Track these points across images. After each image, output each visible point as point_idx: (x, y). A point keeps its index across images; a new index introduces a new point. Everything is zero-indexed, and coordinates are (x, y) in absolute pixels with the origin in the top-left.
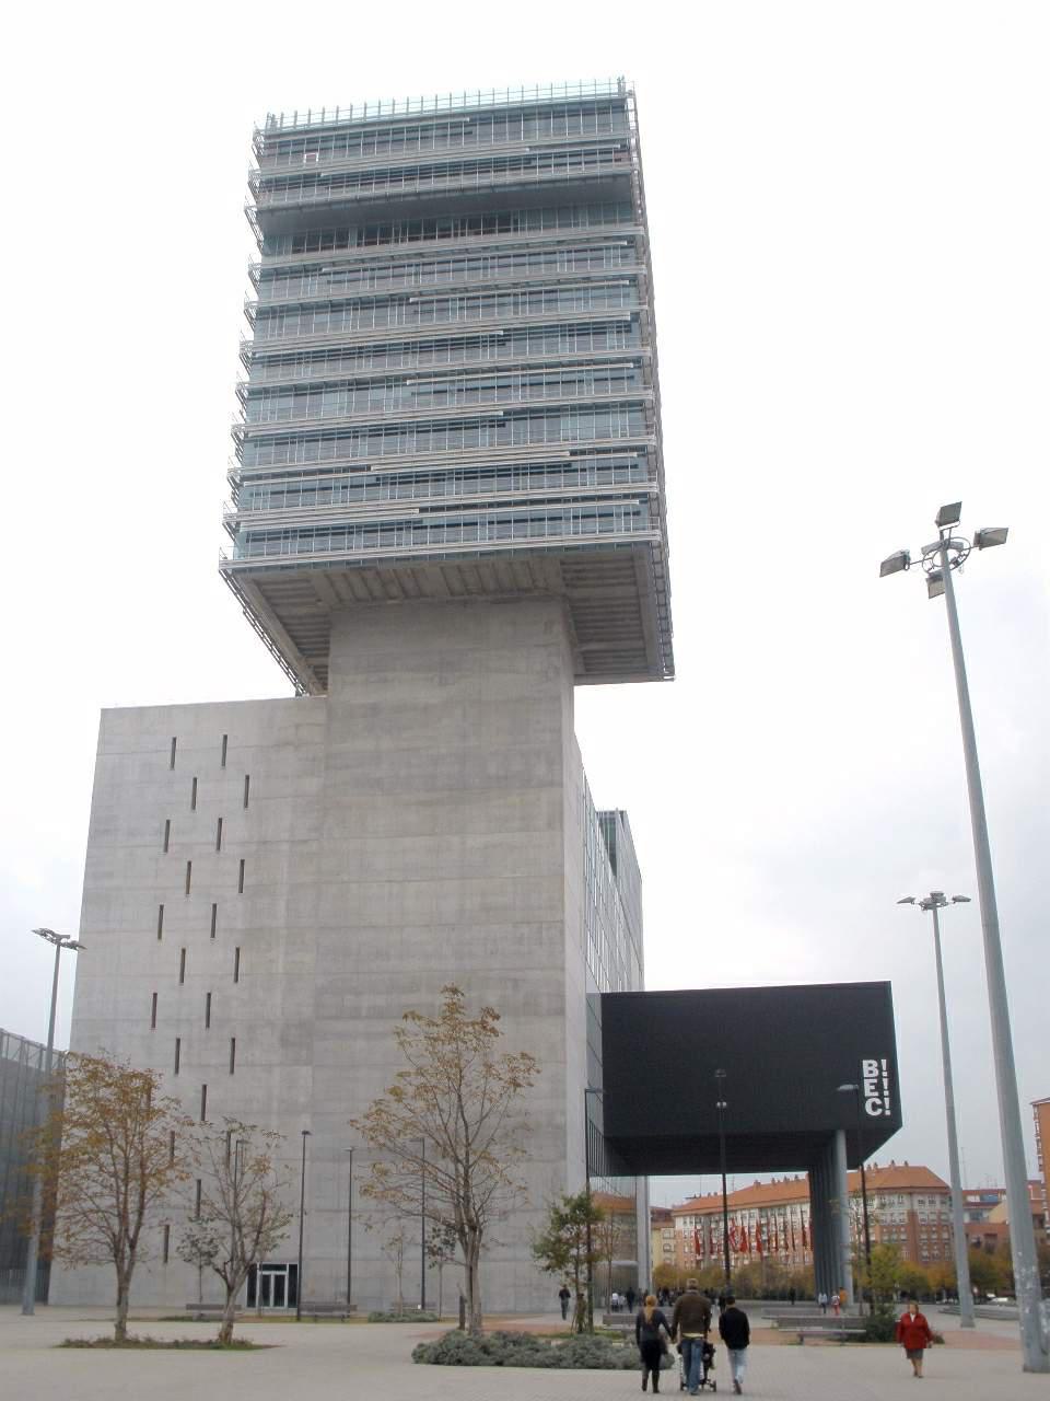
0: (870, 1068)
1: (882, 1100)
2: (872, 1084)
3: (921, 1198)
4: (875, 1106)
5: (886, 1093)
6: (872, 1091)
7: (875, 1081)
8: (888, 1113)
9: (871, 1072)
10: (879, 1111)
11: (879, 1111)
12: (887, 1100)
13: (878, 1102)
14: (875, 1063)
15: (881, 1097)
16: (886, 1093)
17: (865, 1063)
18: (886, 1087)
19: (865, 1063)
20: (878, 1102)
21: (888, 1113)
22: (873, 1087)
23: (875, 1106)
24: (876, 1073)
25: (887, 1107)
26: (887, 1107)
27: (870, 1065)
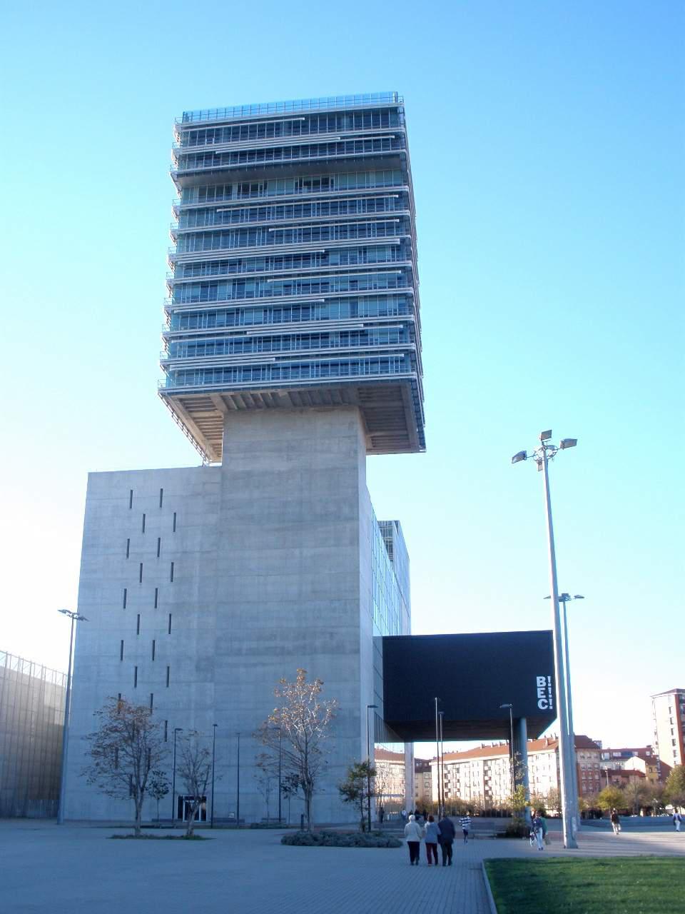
0: (541, 682)
1: (548, 700)
3: (582, 754)
4: (543, 704)
5: (550, 696)
6: (542, 695)
7: (544, 689)
8: (551, 708)
9: (541, 684)
10: (546, 707)
11: (546, 707)
12: (551, 700)
13: (546, 701)
14: (544, 678)
15: (547, 698)
16: (550, 696)
17: (538, 678)
19: (538, 678)
20: (546, 701)
21: (551, 708)
22: (543, 693)
23: (543, 704)
24: (544, 684)
27: (541, 680)
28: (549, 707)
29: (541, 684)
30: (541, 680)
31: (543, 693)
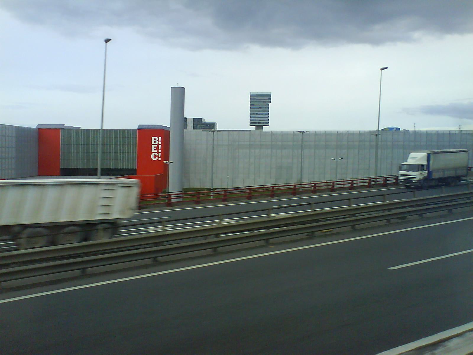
0: (155, 141)
1: (158, 154)
2: (155, 147)
4: (155, 157)
5: (160, 151)
6: (155, 150)
7: (156, 146)
8: (160, 159)
9: (155, 142)
10: (157, 158)
11: (157, 158)
12: (160, 154)
13: (157, 154)
14: (157, 138)
16: (160, 151)
17: (153, 138)
18: (160, 149)
19: (153, 138)
20: (157, 154)
21: (160, 159)
22: (155, 148)
23: (155, 157)
25: (160, 157)
26: (160, 157)
27: (155, 139)
28: (158, 159)
29: (155, 142)
30: (155, 139)
31: (155, 148)
